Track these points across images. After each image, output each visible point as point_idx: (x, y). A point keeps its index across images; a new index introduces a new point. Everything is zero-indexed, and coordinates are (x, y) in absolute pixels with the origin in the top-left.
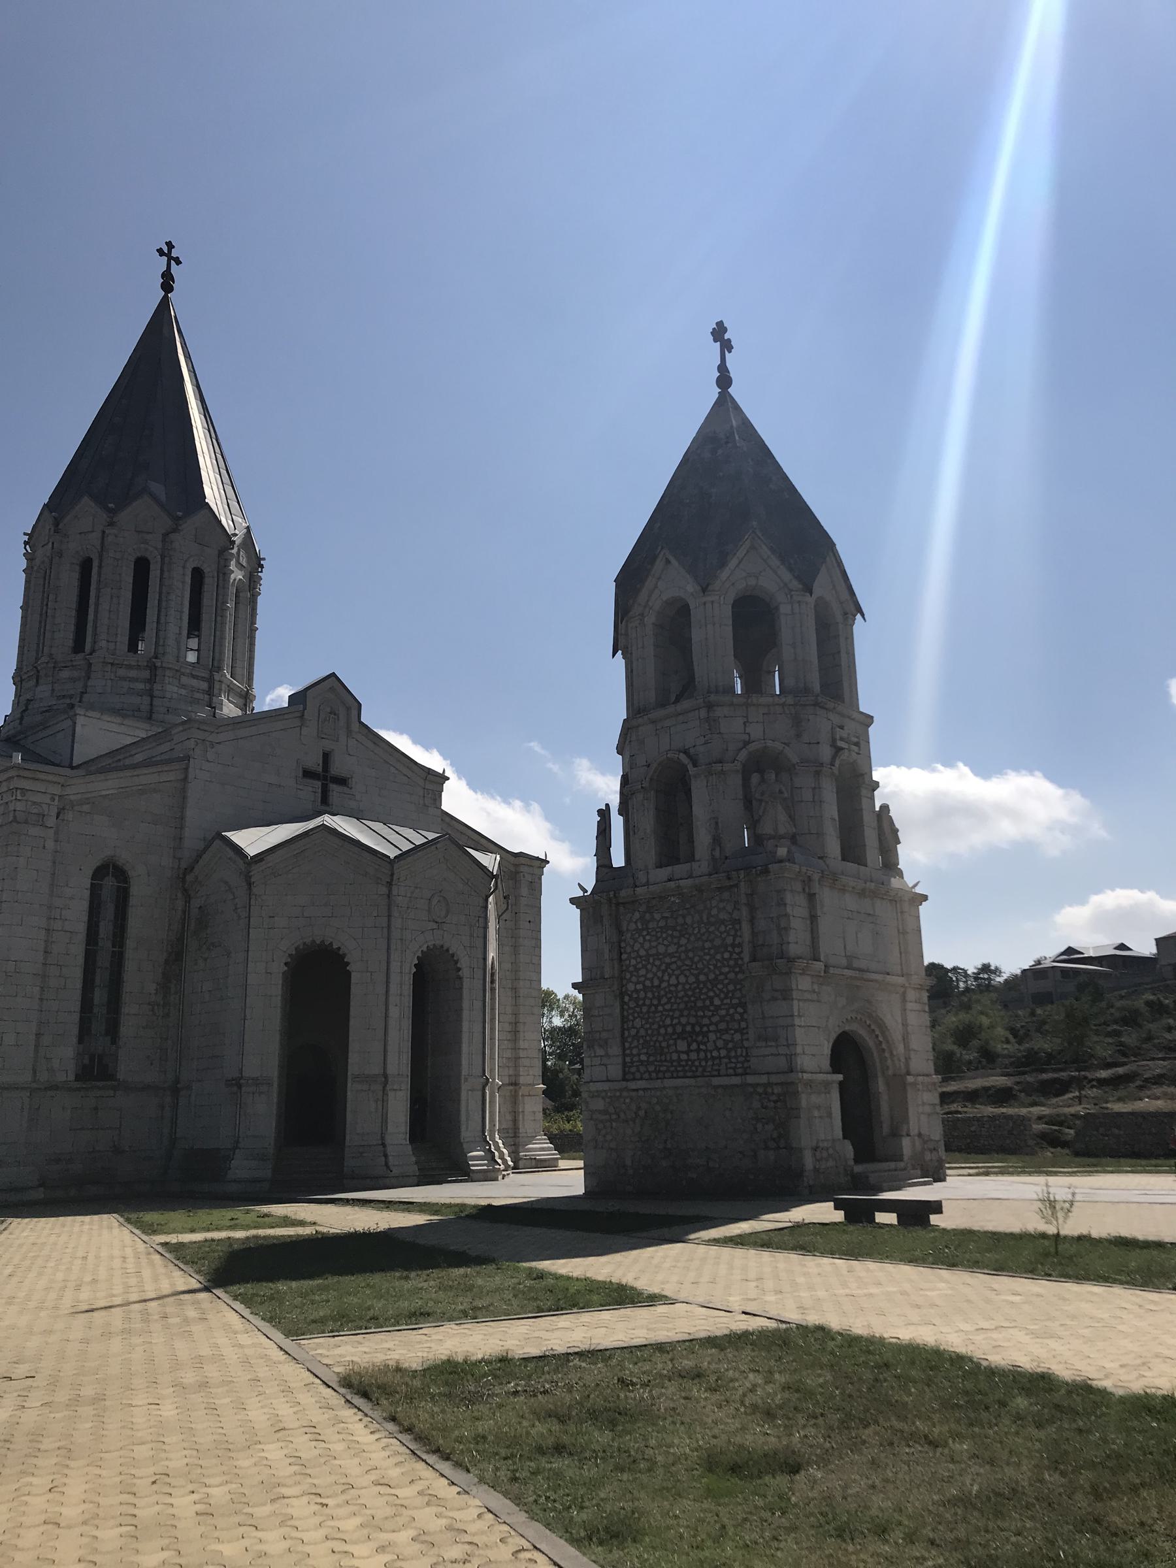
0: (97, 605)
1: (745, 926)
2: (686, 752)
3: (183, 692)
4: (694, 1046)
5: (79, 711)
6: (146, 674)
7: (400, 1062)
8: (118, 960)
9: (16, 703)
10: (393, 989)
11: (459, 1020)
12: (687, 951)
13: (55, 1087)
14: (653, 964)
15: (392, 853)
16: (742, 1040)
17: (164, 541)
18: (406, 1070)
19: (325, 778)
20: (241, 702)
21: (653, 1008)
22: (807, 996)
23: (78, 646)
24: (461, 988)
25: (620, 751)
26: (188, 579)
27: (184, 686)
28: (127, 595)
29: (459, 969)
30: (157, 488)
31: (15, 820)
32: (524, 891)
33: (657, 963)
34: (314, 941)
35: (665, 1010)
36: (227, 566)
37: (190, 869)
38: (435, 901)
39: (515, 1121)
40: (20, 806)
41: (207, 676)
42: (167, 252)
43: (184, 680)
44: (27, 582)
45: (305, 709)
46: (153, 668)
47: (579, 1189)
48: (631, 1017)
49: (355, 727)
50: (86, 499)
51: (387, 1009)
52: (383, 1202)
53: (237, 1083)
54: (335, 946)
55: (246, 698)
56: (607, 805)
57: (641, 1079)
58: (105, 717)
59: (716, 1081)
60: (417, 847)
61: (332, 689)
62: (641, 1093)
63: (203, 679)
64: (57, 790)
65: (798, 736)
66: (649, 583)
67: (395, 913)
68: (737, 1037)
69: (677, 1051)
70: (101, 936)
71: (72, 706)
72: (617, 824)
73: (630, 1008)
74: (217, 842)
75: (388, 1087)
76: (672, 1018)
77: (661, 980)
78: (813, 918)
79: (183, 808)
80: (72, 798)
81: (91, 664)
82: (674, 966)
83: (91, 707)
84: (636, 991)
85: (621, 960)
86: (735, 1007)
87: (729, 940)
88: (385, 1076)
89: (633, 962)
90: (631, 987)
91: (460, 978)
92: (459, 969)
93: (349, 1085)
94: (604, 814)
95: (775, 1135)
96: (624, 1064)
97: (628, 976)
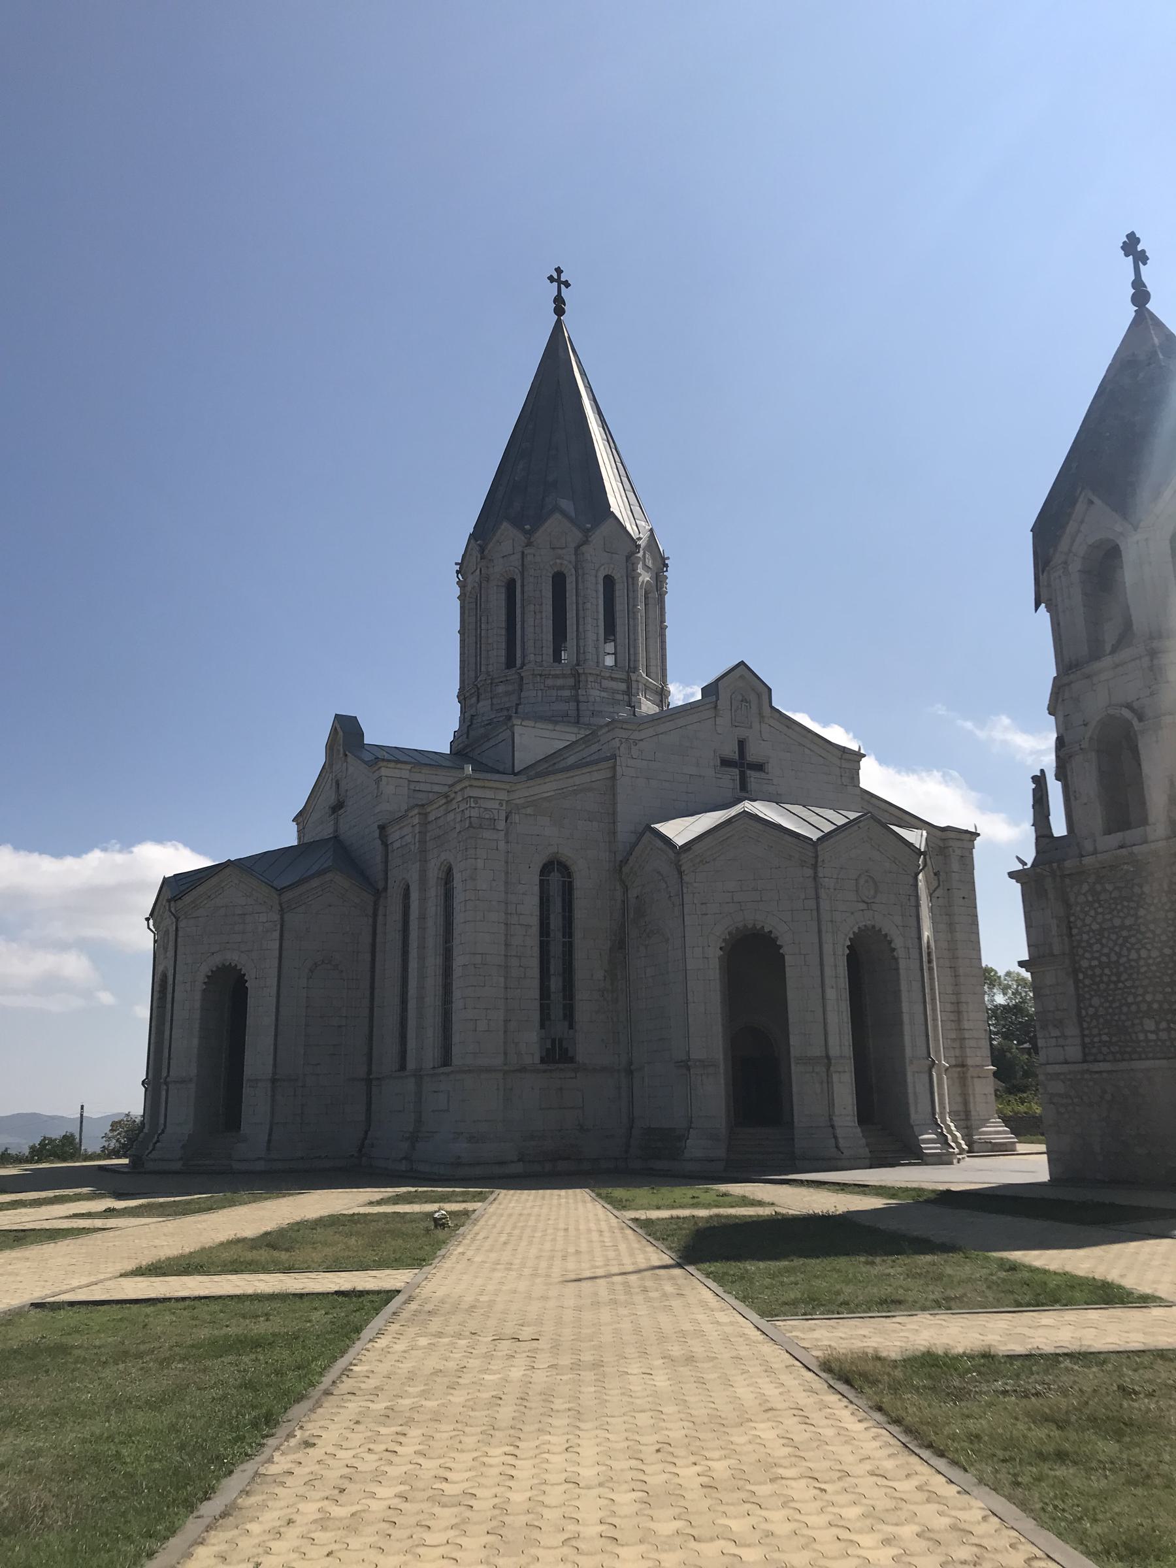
0: (523, 622)
2: (1129, 706)
3: (604, 694)
5: (517, 721)
6: (571, 681)
7: (841, 1043)
9: (462, 720)
13: (523, 1070)
15: (814, 835)
17: (576, 554)
18: (848, 1051)
19: (742, 765)
20: (657, 698)
21: (1112, 986)
23: (510, 662)
24: (897, 969)
25: (1052, 711)
26: (601, 588)
27: (605, 690)
28: (548, 608)
29: (894, 950)
30: (566, 504)
31: (471, 826)
32: (955, 866)
33: (1114, 937)
34: (745, 926)
35: (1126, 987)
36: (634, 570)
37: (624, 862)
38: (862, 881)
39: (966, 1103)
40: (474, 813)
41: (624, 676)
42: (558, 279)
43: (605, 683)
44: (462, 607)
45: (718, 699)
46: (576, 676)
47: (1044, 1176)
48: (1087, 996)
49: (766, 711)
50: (505, 525)
51: (823, 992)
53: (685, 1065)
54: (766, 930)
55: (662, 694)
56: (1042, 771)
57: (1104, 1060)
58: (538, 725)
60: (839, 828)
61: (741, 677)
62: (1105, 1075)
63: (622, 681)
64: (503, 796)
66: (1071, 527)
69: (1146, 1032)
70: (552, 927)
71: (509, 718)
72: (1055, 789)
73: (1085, 986)
74: (648, 834)
75: (832, 1068)
76: (1135, 995)
79: (614, 804)
80: (518, 801)
81: (522, 678)
82: (1133, 940)
83: (526, 717)
84: (1091, 967)
85: (1071, 936)
88: (828, 1057)
89: (1085, 937)
90: (1085, 964)
91: (896, 959)
92: (894, 950)
93: (793, 1067)
94: (1039, 781)
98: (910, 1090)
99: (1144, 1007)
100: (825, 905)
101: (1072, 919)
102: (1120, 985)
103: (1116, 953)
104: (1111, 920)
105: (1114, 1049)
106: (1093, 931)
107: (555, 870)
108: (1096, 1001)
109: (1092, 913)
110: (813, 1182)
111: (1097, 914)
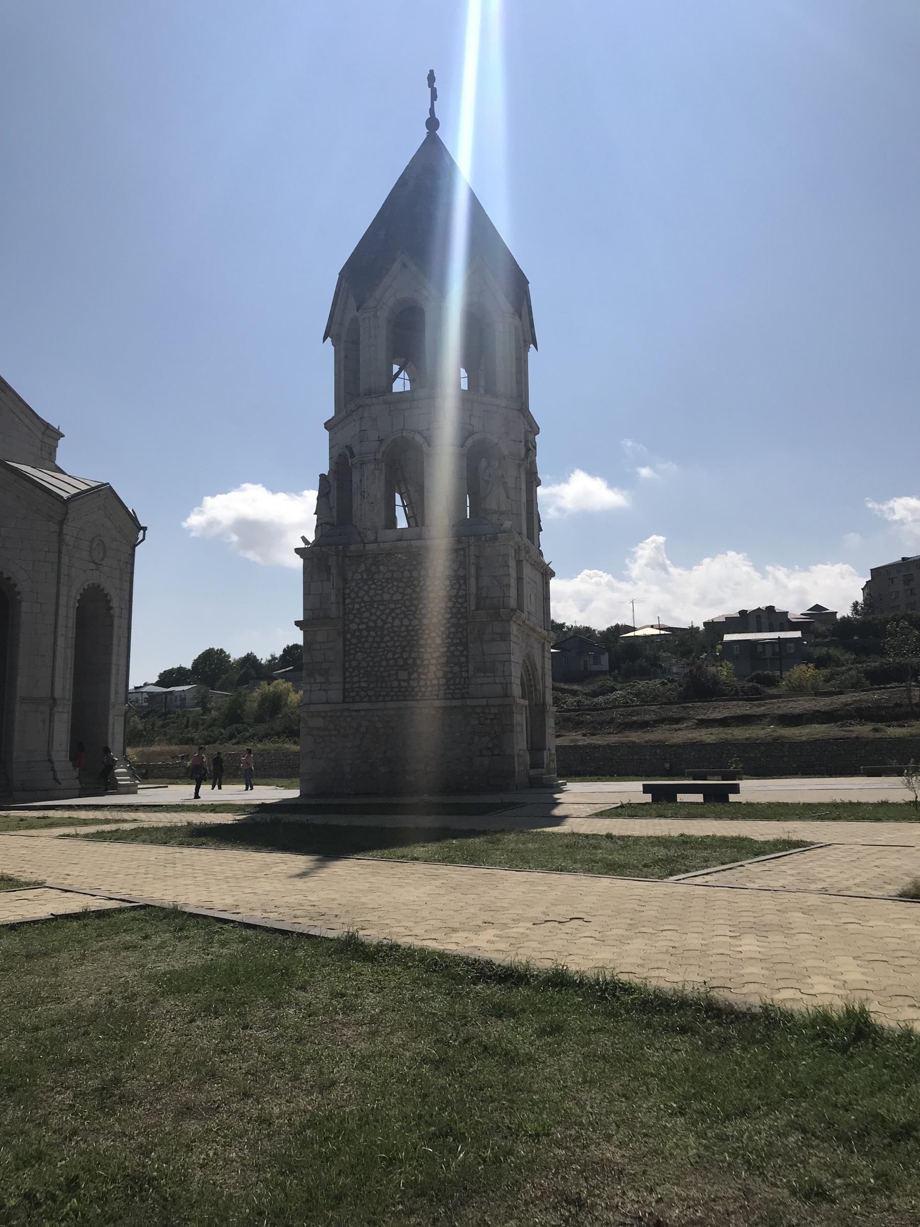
1: (473, 582)
7: (64, 688)
10: (61, 621)
14: (377, 608)
15: (65, 496)
16: (461, 672)
18: (69, 694)
21: (375, 645)
24: (112, 625)
29: (111, 608)
33: (382, 608)
35: (387, 646)
38: (95, 545)
51: (55, 639)
52: (129, 806)
57: (361, 702)
67: (64, 551)
69: (399, 681)
76: (394, 653)
78: (520, 579)
82: (398, 611)
84: (358, 629)
85: (344, 604)
90: (354, 627)
91: (111, 617)
92: (111, 608)
95: (490, 745)
96: (344, 689)
97: (351, 617)
98: (110, 731)
99: (401, 662)
100: (65, 560)
101: (347, 591)
102: (383, 645)
103: (382, 620)
104: (381, 595)
105: (371, 693)
106: (365, 602)
108: (359, 656)
109: (366, 588)
110: (90, 806)
111: (370, 589)
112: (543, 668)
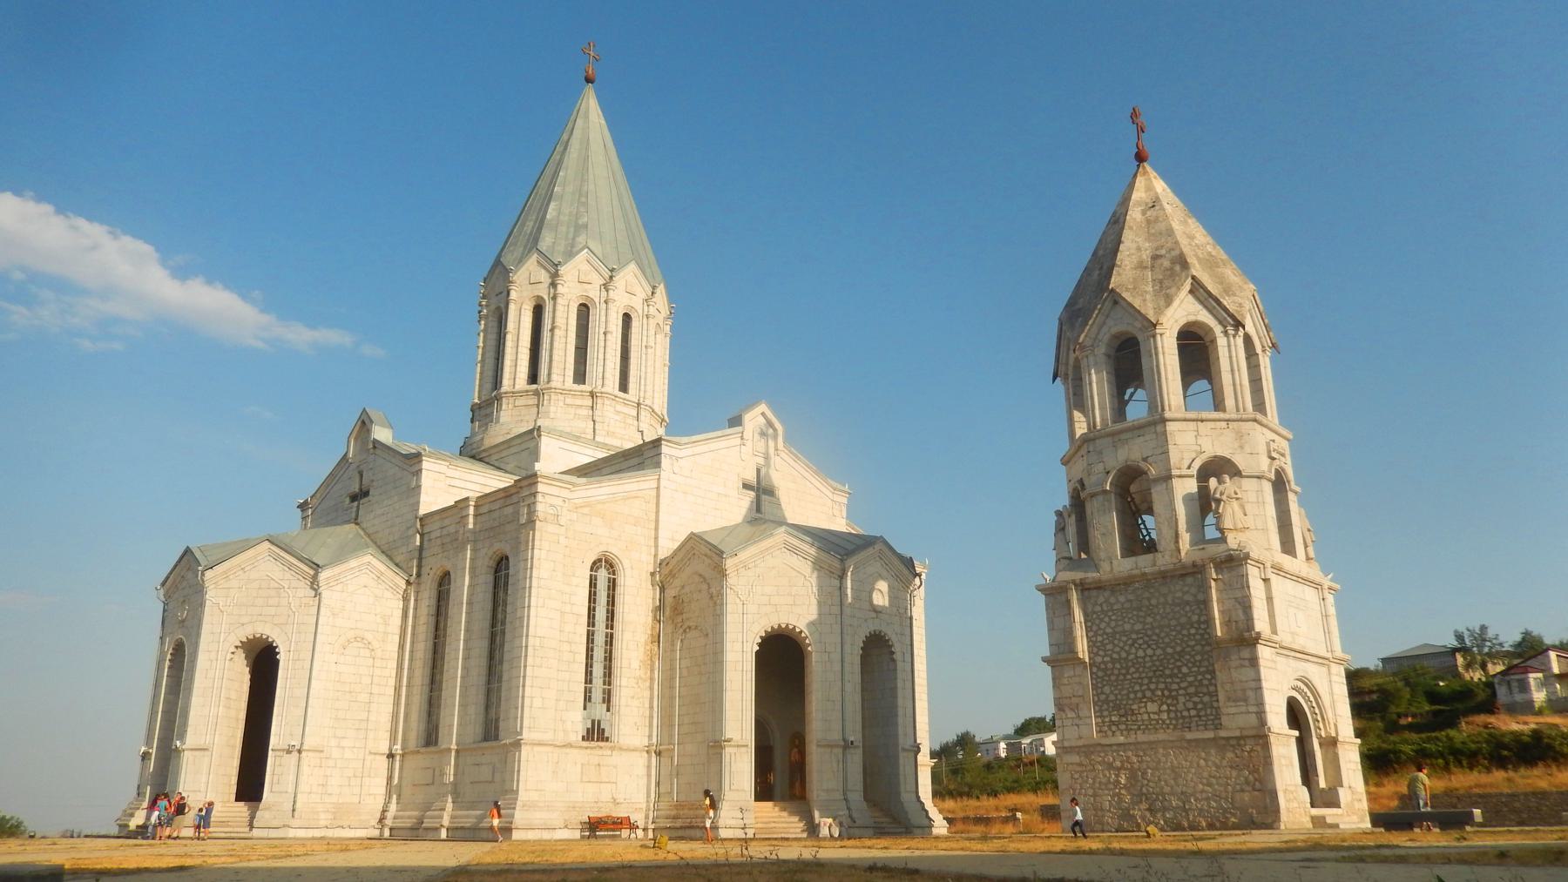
4: (1165, 707)
8: (610, 640)
11: (895, 697)
12: (1153, 628)
13: (570, 745)
22: (1270, 664)
23: (533, 378)
24: (895, 670)
59: (1189, 736)
64: (565, 493)
65: (1242, 447)
68: (1206, 699)
77: (1128, 653)
78: (1270, 599)
86: (1203, 674)
87: (1195, 618)
91: (894, 660)
99: (1148, 694)
107: (605, 563)
108: (1107, 689)
112: (1332, 694)
